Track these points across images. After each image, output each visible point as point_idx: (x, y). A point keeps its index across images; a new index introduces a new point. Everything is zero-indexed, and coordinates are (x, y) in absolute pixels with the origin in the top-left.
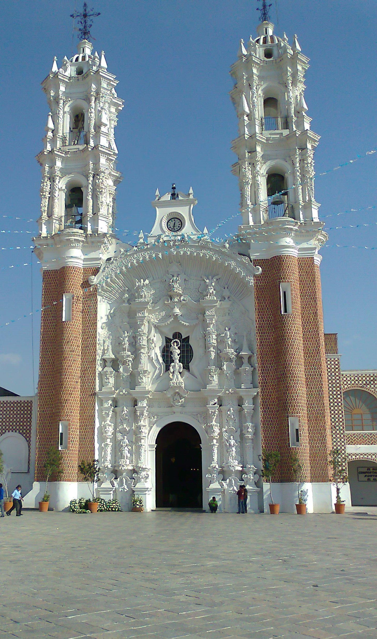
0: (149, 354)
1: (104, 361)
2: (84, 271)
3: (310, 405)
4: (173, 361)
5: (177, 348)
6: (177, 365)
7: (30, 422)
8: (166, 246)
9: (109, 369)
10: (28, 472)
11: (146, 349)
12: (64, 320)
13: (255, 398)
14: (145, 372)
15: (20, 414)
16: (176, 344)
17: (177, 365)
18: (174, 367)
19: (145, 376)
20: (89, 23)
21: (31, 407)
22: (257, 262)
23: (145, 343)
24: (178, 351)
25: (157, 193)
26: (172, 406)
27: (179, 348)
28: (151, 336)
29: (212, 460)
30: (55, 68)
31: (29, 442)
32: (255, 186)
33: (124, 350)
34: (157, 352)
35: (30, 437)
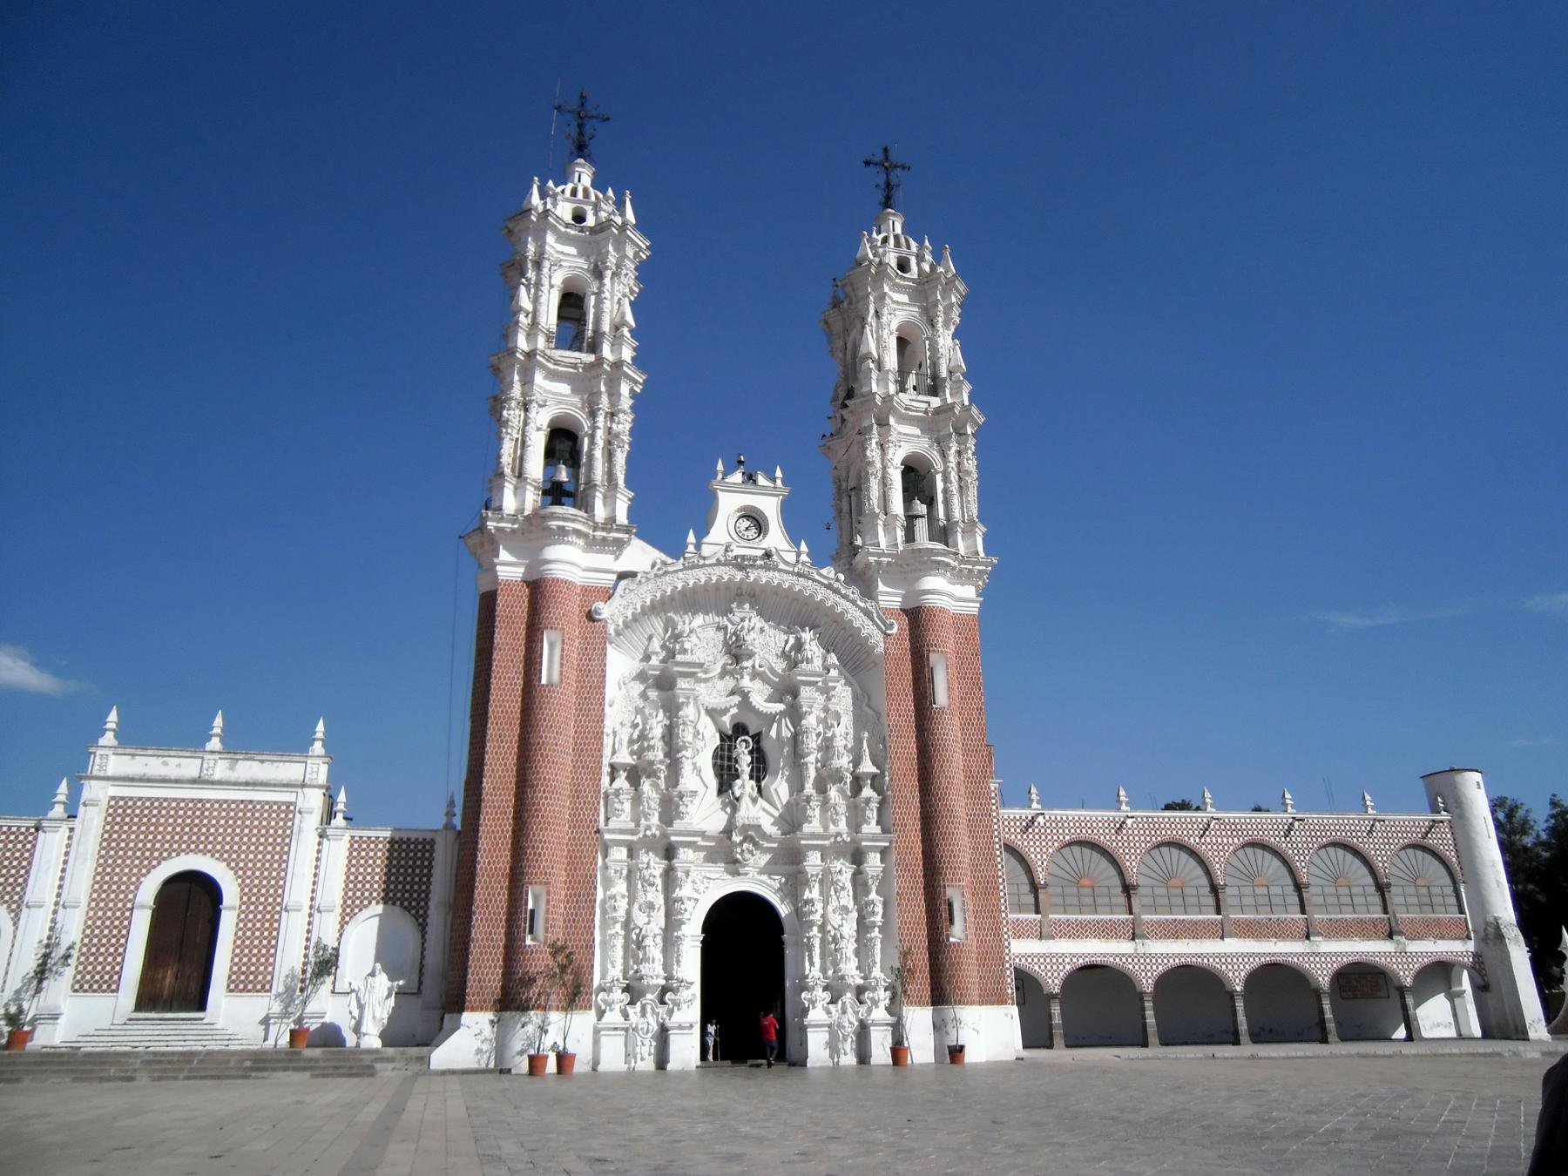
1: (614, 769)
3: (975, 867)
4: (738, 777)
7: (429, 883)
8: (741, 564)
9: (622, 782)
10: (419, 992)
12: (544, 681)
14: (694, 793)
15: (405, 867)
18: (743, 786)
20: (588, 130)
21: (431, 851)
23: (689, 738)
25: (720, 467)
28: (700, 727)
30: (535, 199)
31: (423, 928)
32: (884, 483)
33: (651, 748)
34: (706, 761)
35: (425, 916)
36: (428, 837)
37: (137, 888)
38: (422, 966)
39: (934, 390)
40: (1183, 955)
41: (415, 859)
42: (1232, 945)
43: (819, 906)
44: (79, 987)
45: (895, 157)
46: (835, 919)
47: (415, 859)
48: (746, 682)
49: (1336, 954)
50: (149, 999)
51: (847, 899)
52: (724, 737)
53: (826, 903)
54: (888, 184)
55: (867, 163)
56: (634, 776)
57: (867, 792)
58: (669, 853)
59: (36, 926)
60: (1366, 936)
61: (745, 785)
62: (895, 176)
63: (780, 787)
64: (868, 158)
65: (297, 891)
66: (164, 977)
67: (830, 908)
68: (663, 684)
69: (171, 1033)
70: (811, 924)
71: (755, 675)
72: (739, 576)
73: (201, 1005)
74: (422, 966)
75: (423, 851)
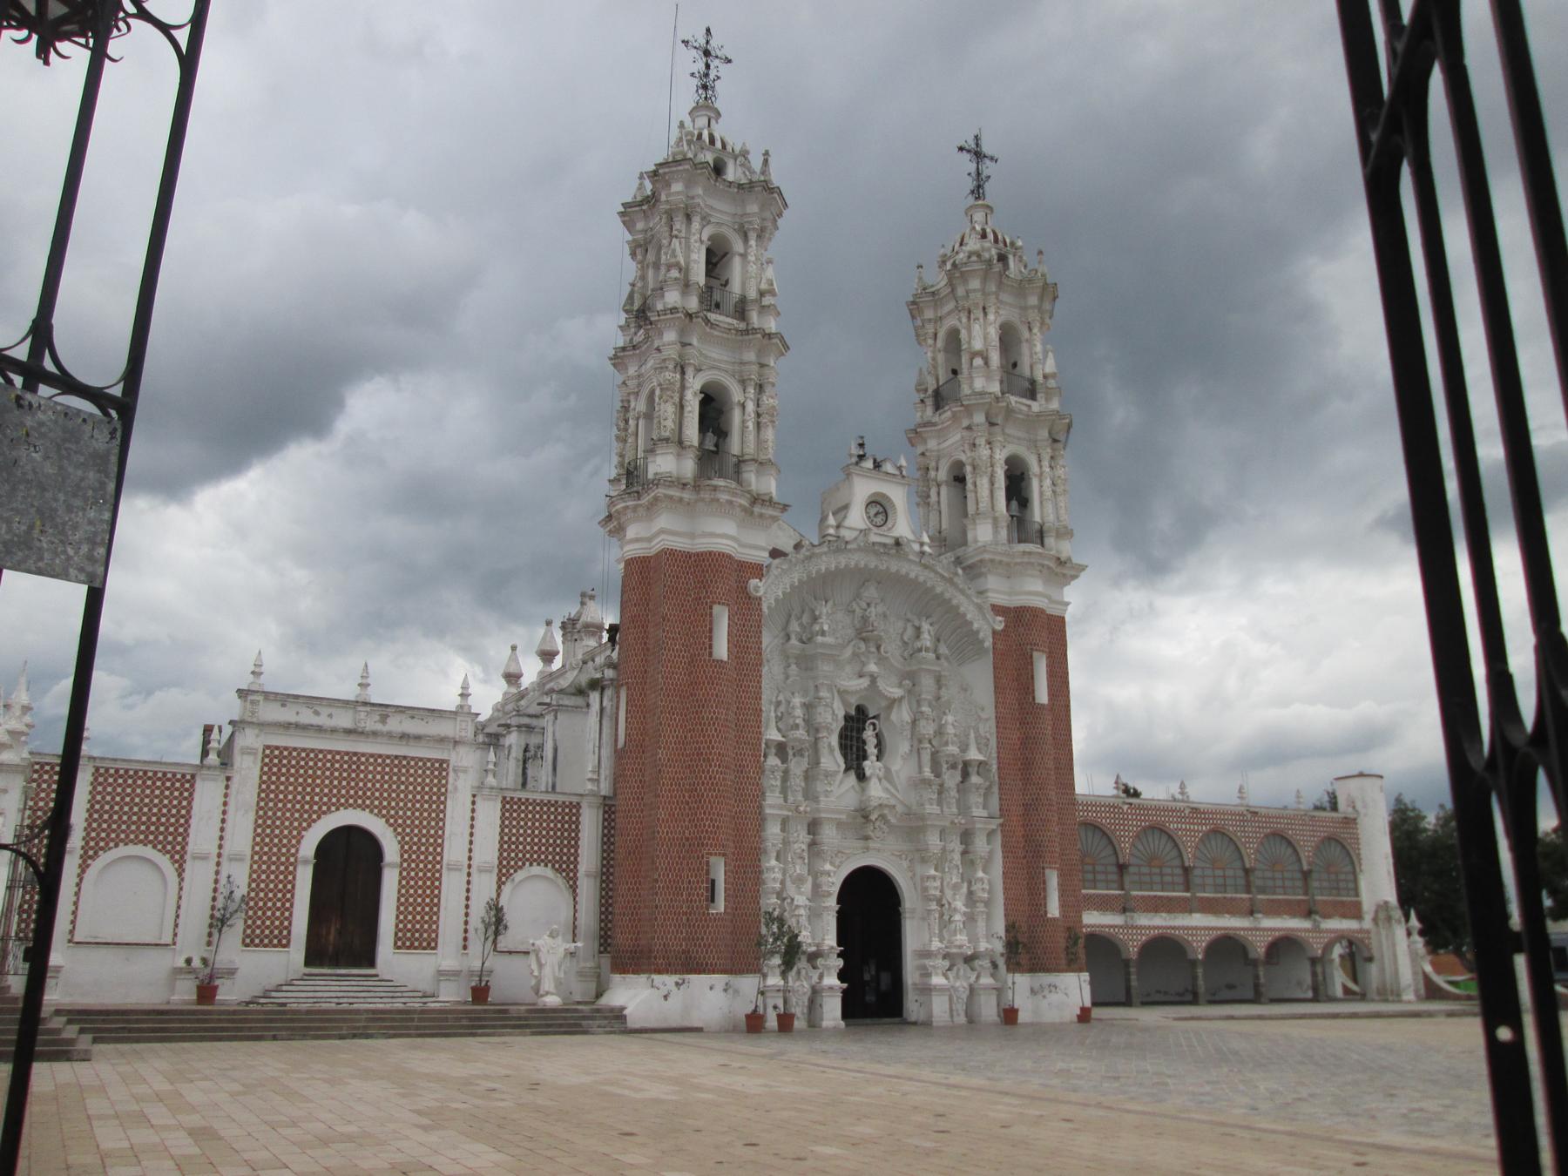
4: (865, 758)
7: (576, 847)
13: (990, 834)
15: (555, 829)
21: (578, 815)
22: (998, 610)
26: (867, 838)
29: (914, 936)
31: (574, 889)
35: (575, 879)
36: (575, 800)
37: (299, 842)
38: (575, 927)
39: (1032, 393)
40: (1158, 928)
41: (563, 822)
42: (1198, 920)
44: (249, 941)
45: (986, 148)
47: (563, 822)
49: (1149, 928)
50: (315, 955)
54: (979, 174)
55: (961, 149)
56: (781, 750)
57: (975, 779)
58: (813, 827)
59: (199, 877)
60: (1293, 915)
61: (870, 766)
62: (988, 168)
64: (962, 143)
65: (454, 850)
66: (328, 933)
69: (336, 989)
73: (371, 963)
74: (575, 927)
75: (571, 814)
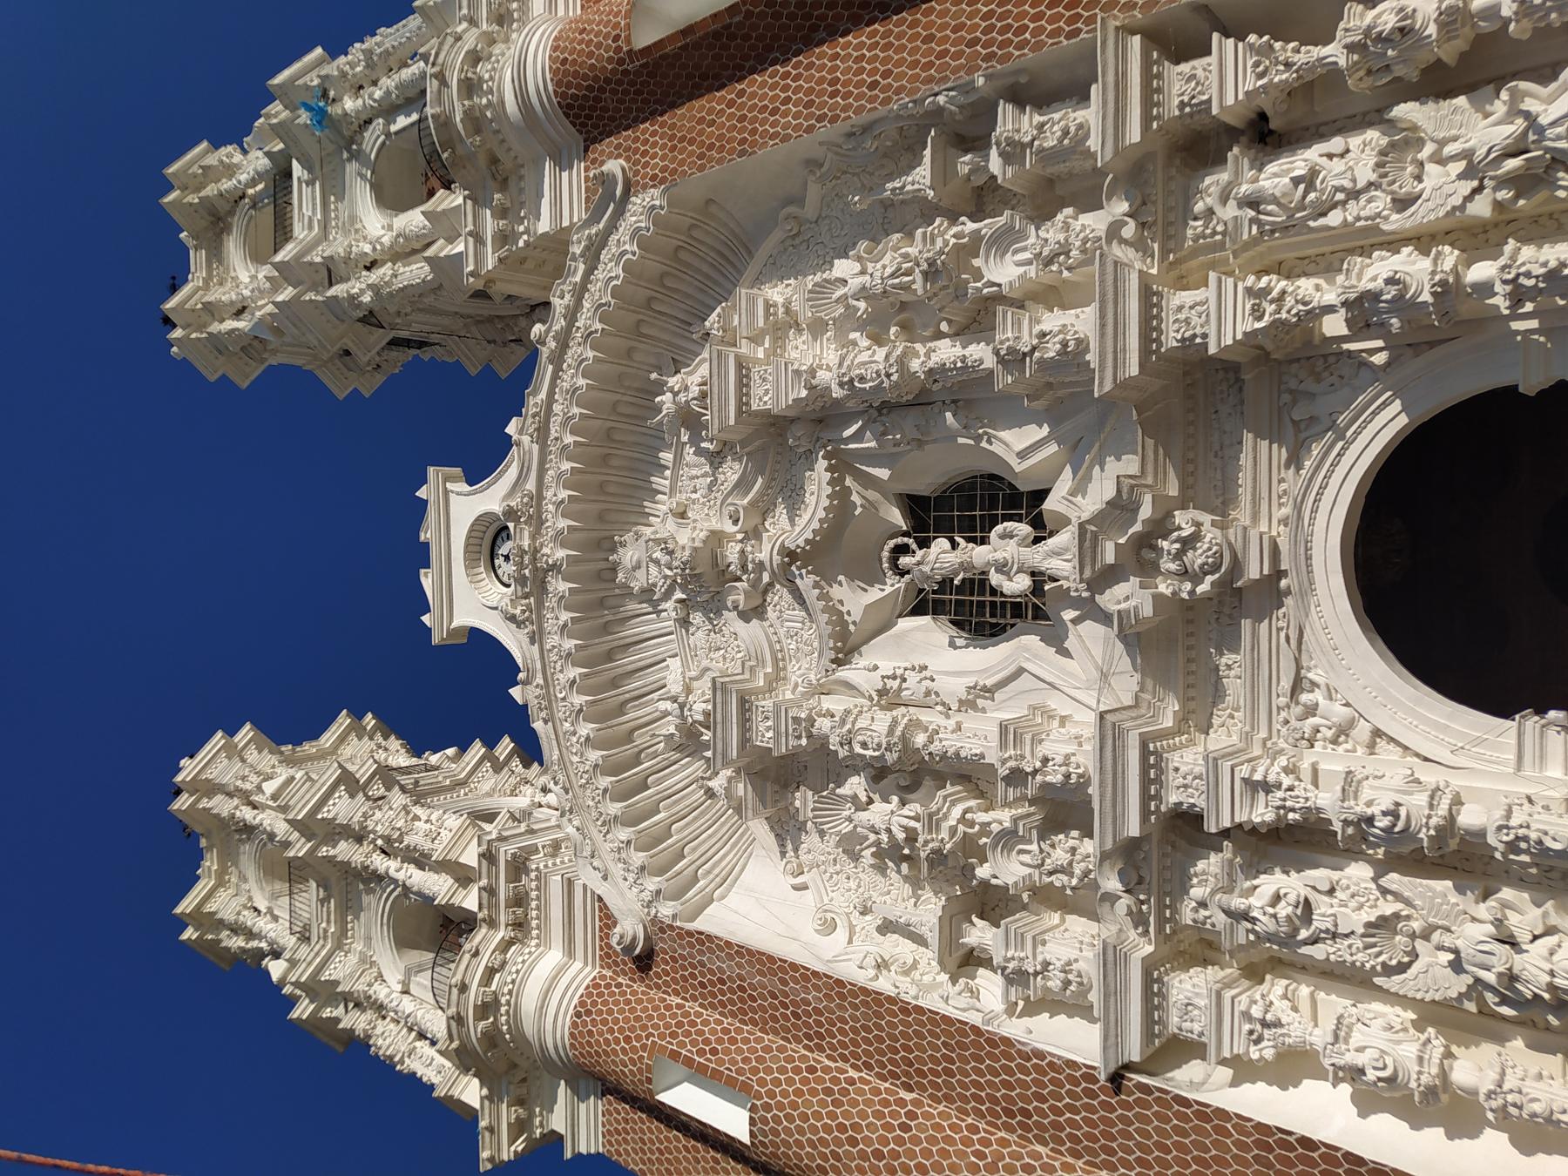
0: (955, 706)
2: (609, 967)
5: (920, 553)
6: (999, 555)
11: (925, 716)
16: (905, 561)
17: (1004, 556)
18: (1002, 568)
19: (1037, 740)
24: (942, 544)
27: (924, 544)
43: (1374, 272)
46: (1441, 188)
48: (766, 552)
51: (1349, 158)
52: (925, 601)
53: (1370, 240)
63: (1018, 446)
67: (1395, 222)
68: (788, 779)
70: (1447, 291)
71: (754, 534)
72: (559, 586)
